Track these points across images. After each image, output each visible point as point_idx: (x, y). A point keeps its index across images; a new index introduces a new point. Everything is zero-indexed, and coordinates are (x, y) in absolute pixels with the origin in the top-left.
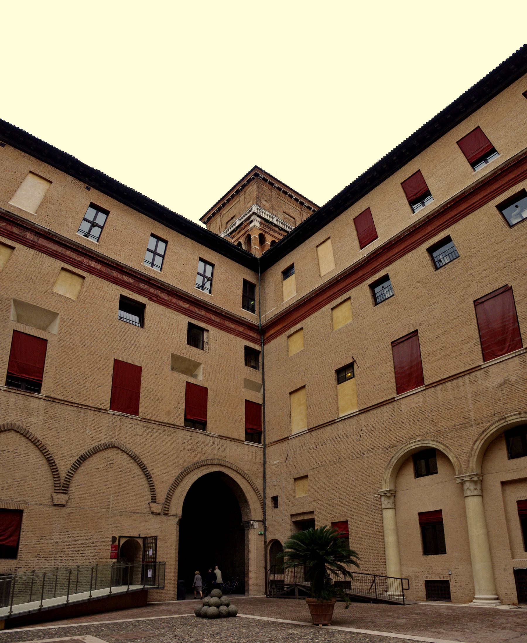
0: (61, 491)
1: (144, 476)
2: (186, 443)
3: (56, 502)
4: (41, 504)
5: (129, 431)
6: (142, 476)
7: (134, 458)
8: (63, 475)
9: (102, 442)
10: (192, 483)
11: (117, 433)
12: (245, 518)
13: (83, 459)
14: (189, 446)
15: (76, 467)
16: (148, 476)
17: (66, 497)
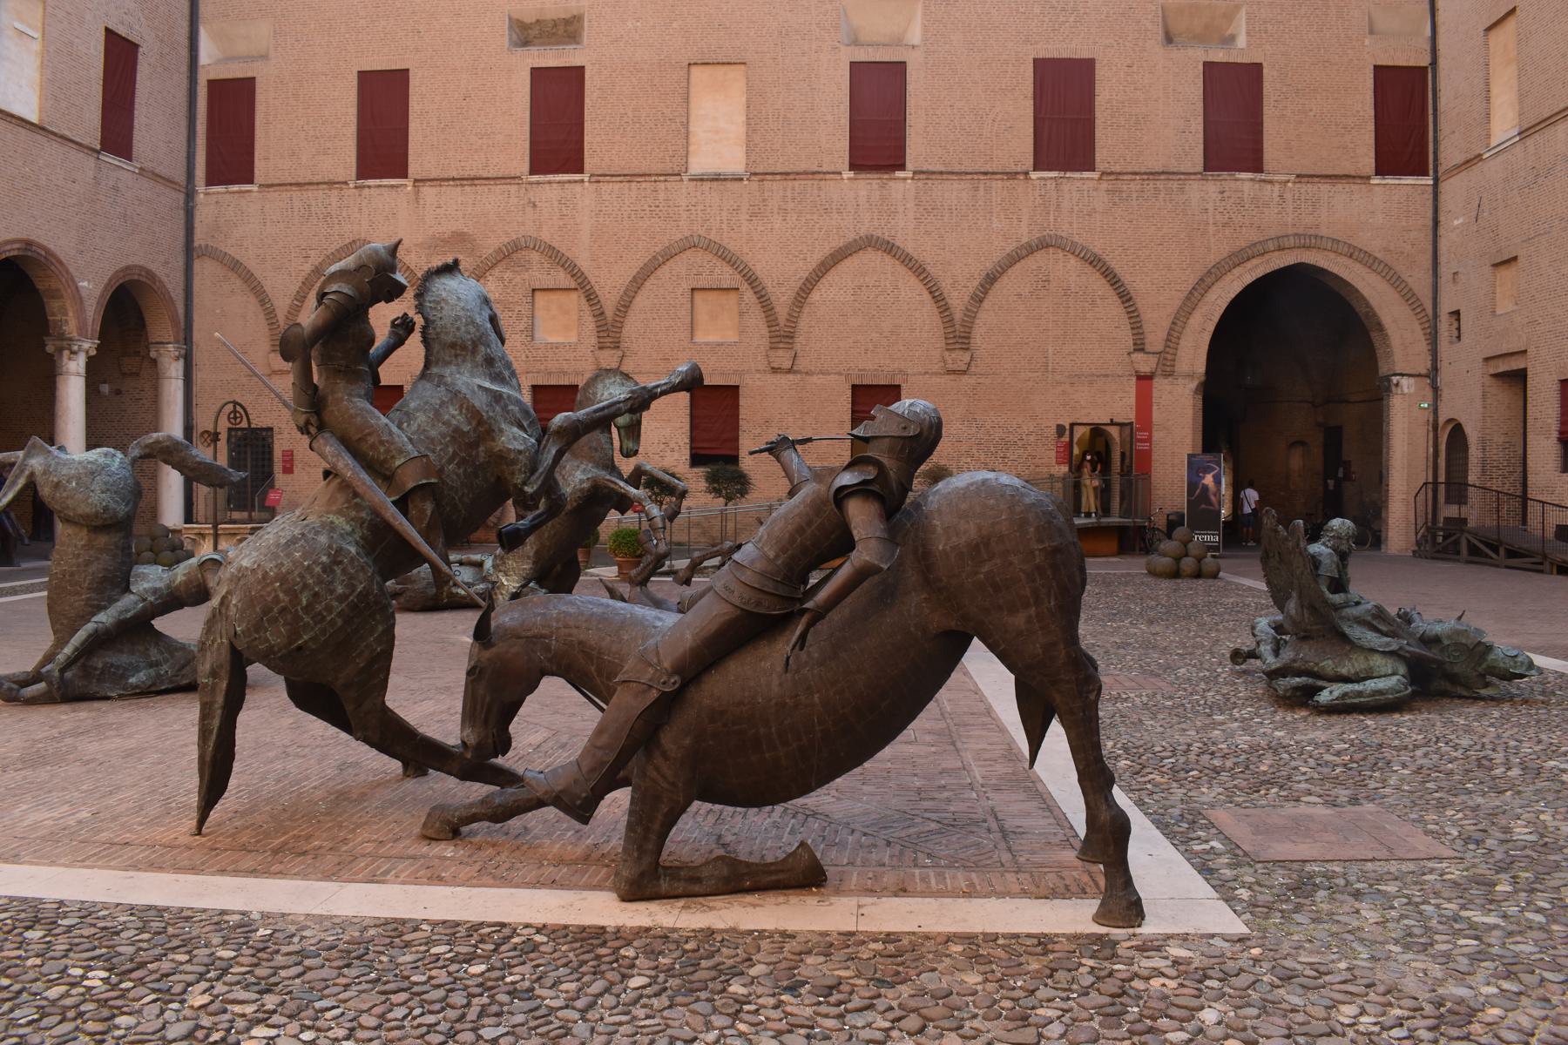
0: (958, 346)
1: (1116, 298)
2: (1211, 209)
3: (950, 367)
4: (926, 373)
5: (1076, 208)
6: (1113, 298)
7: (1095, 262)
8: (958, 316)
9: (1025, 240)
10: (1229, 300)
11: (1052, 217)
12: (1383, 370)
13: (991, 280)
14: (1218, 217)
15: (978, 299)
16: (1125, 297)
17: (966, 357)
